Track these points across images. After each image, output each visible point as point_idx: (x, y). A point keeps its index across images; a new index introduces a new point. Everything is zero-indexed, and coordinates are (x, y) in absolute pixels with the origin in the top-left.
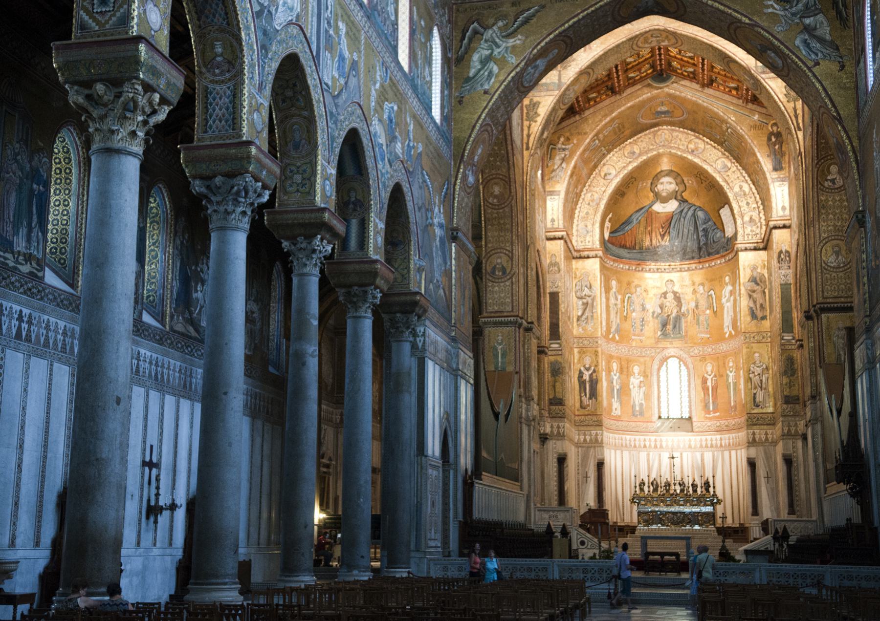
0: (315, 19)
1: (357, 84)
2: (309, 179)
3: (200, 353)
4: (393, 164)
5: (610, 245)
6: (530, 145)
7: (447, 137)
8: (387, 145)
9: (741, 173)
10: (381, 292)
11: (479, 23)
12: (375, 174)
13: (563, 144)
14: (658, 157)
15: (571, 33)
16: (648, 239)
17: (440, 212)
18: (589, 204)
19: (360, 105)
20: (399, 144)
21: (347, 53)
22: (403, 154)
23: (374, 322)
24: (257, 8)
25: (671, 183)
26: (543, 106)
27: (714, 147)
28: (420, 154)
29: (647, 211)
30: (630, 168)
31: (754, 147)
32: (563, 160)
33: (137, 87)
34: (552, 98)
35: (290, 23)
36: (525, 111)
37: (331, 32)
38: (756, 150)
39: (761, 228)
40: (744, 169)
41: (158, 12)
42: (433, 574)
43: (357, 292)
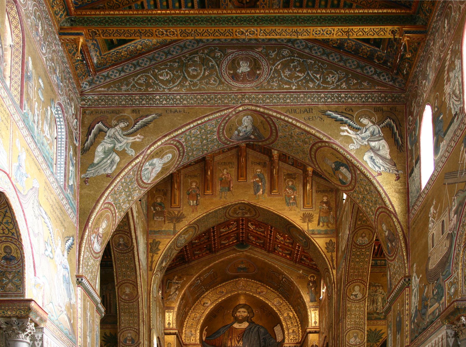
5: (206, 344)
6: (153, 268)
9: (289, 307)
13: (176, 280)
14: (238, 295)
15: (183, 140)
16: (229, 343)
18: (193, 319)
25: (245, 312)
26: (163, 245)
27: (273, 291)
29: (230, 327)
30: (220, 300)
31: (299, 289)
32: (177, 289)
34: (169, 240)
36: (150, 247)
38: (300, 290)
39: (299, 336)
40: (290, 304)
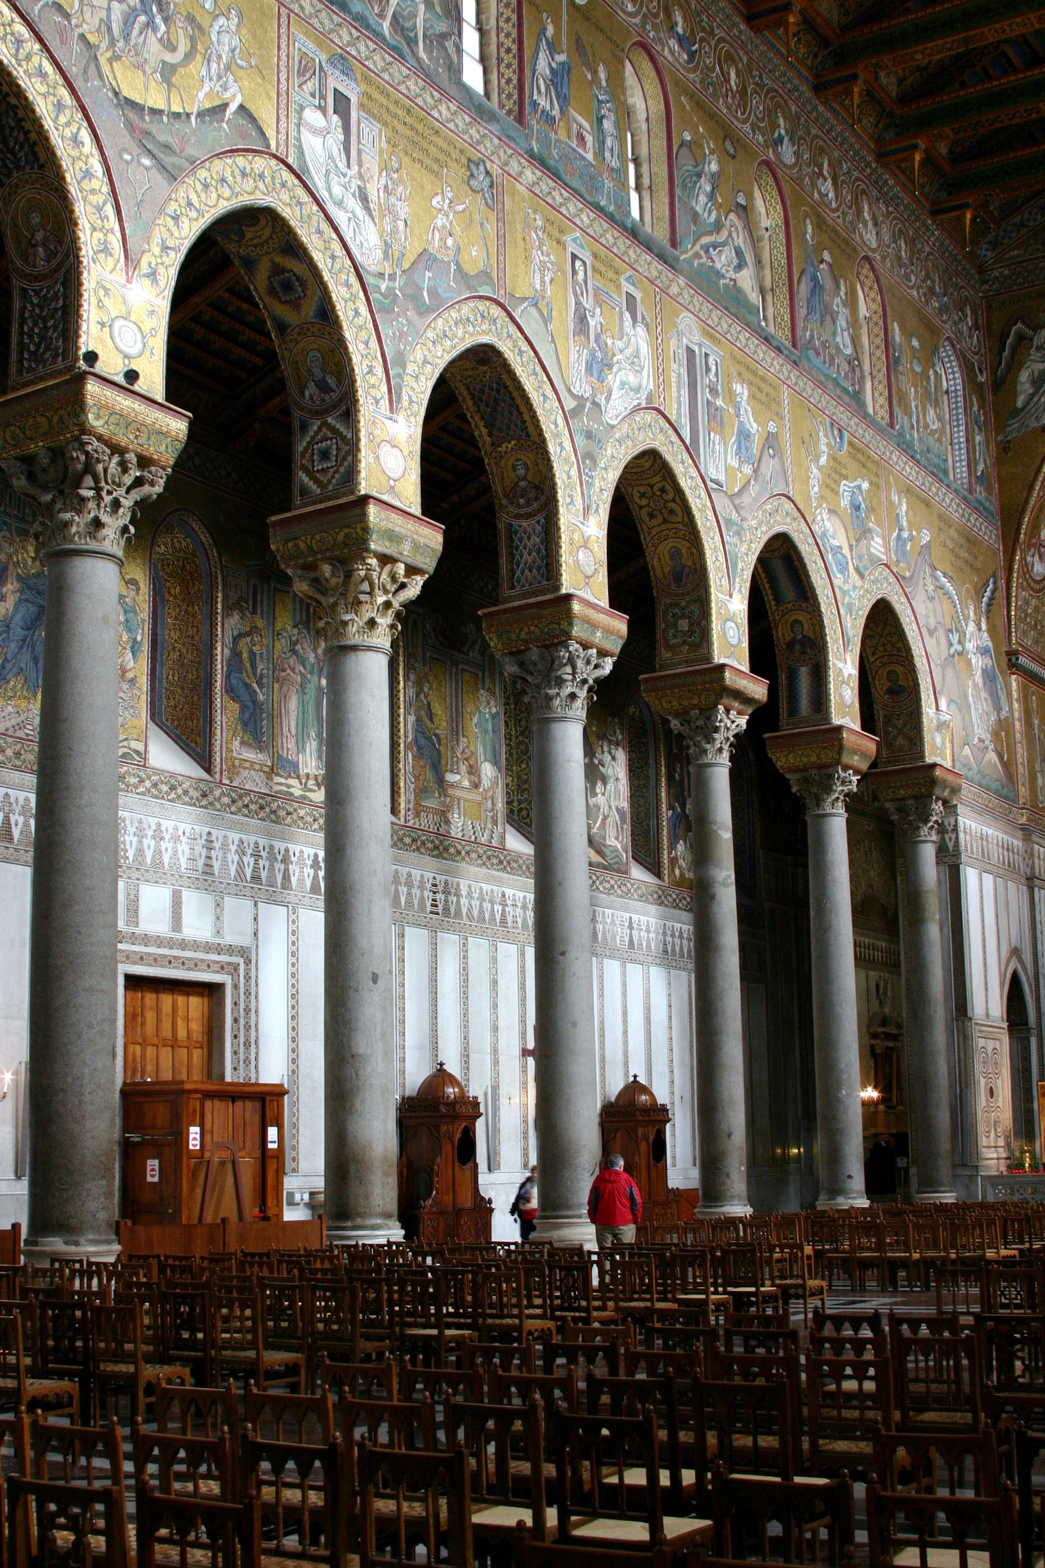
0: (685, 392)
1: (778, 467)
2: (699, 624)
3: (608, 886)
4: (866, 574)
7: (985, 509)
8: (851, 547)
10: (856, 772)
11: (1024, 323)
12: (831, 594)
17: (980, 629)
19: (789, 498)
20: (879, 540)
21: (755, 425)
22: (888, 550)
23: (848, 821)
24: (570, 404)
28: (928, 545)
33: (369, 561)
35: (637, 409)
37: (719, 402)
41: (399, 454)
42: (991, 1199)
43: (817, 778)
